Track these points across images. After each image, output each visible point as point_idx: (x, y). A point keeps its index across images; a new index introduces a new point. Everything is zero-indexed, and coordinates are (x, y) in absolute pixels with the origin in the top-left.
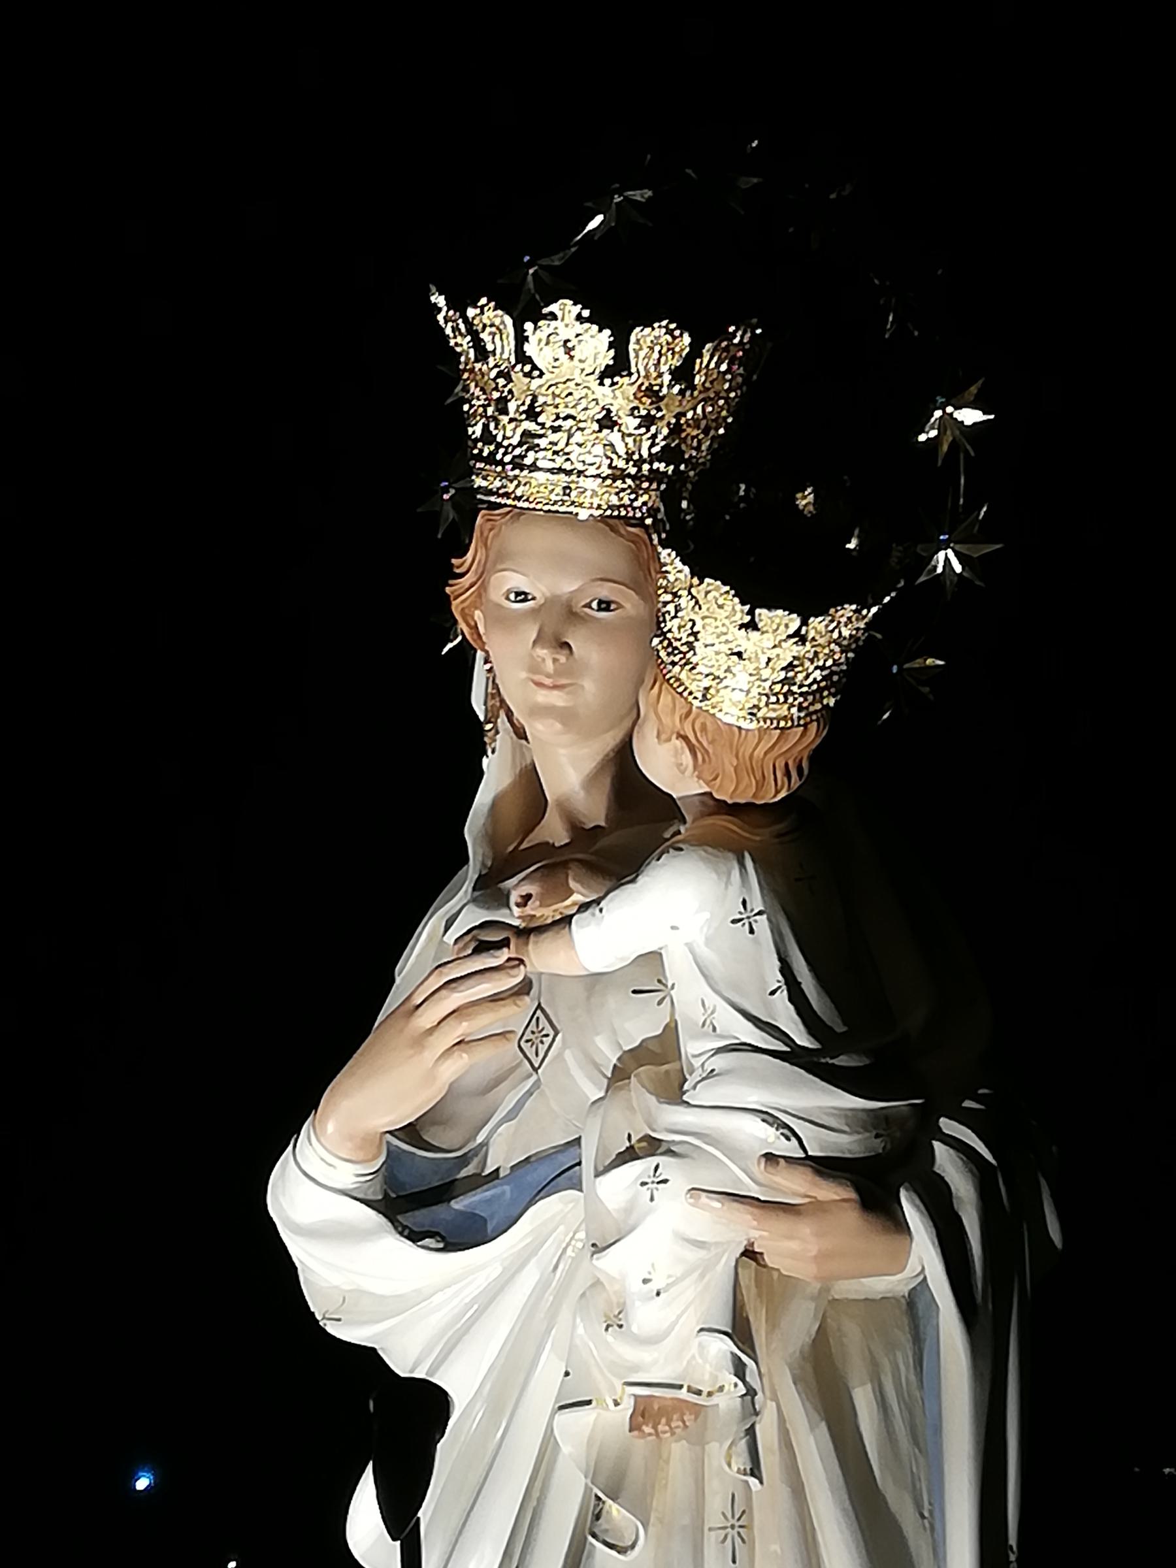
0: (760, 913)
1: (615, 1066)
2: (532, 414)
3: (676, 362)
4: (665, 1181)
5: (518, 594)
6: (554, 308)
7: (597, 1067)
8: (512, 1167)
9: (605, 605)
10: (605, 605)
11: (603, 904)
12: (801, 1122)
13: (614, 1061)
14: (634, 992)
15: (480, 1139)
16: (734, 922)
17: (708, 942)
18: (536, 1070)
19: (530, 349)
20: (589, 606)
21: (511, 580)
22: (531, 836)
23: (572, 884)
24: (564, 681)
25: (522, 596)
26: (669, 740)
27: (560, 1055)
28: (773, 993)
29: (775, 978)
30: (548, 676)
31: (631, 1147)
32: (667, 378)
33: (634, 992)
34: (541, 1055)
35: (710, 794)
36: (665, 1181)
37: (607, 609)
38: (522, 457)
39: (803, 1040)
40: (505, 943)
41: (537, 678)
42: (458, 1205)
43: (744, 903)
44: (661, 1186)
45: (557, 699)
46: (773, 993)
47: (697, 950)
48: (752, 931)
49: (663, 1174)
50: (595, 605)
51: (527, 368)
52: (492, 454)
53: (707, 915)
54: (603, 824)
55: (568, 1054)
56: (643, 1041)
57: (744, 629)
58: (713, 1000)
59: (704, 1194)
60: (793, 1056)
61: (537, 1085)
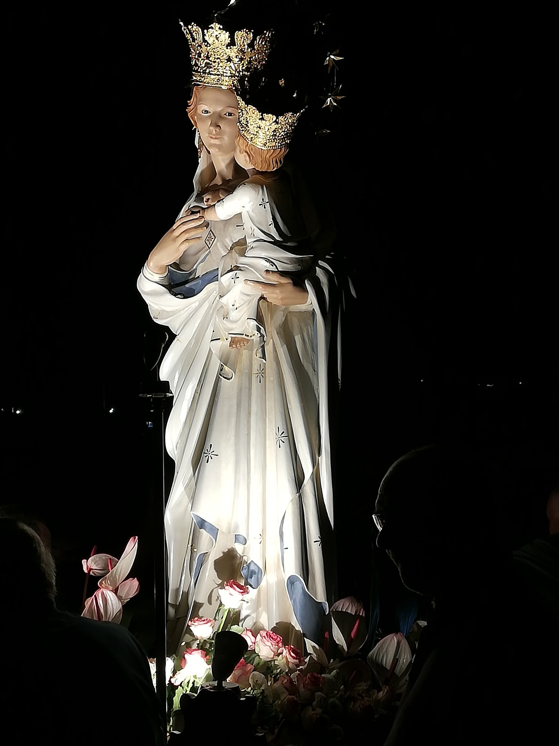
0: (267, 202)
1: (231, 247)
3: (249, 42)
4: (238, 278)
6: (212, 25)
7: (226, 247)
8: (202, 275)
9: (230, 114)
10: (230, 114)
11: (224, 200)
13: (231, 245)
14: (237, 226)
15: (194, 268)
16: (260, 205)
18: (209, 248)
19: (206, 38)
20: (226, 114)
24: (218, 137)
25: (207, 112)
27: (216, 244)
28: (270, 225)
30: (214, 135)
32: (246, 46)
33: (237, 226)
34: (211, 244)
36: (238, 278)
37: (231, 116)
38: (205, 70)
39: (278, 238)
40: (199, 212)
41: (211, 136)
42: (187, 286)
43: (263, 199)
44: (238, 279)
45: (217, 142)
46: (270, 225)
47: (249, 213)
48: (265, 208)
50: (227, 114)
51: (206, 44)
52: (198, 69)
53: (252, 203)
54: (231, 178)
55: (218, 244)
59: (249, 281)
60: (275, 243)
61: (210, 252)
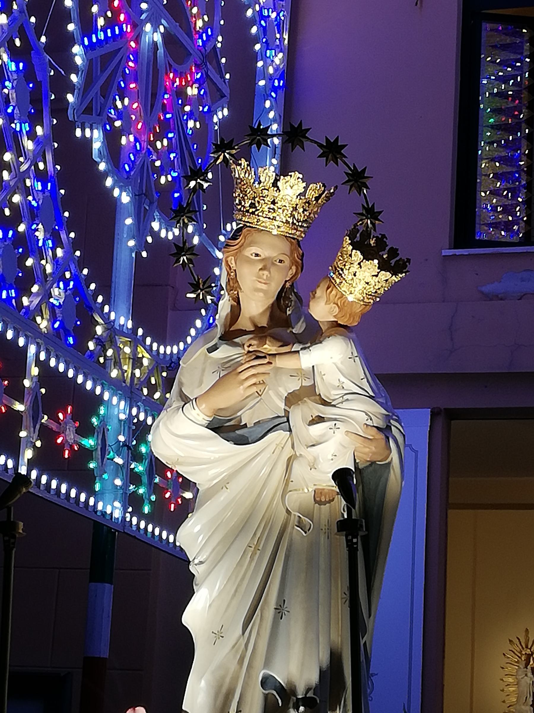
0: (356, 357)
1: (286, 397)
2: (274, 203)
3: (317, 195)
4: (339, 428)
5: (256, 254)
6: (293, 174)
7: (281, 396)
8: (254, 424)
9: (281, 261)
10: (281, 261)
11: (310, 348)
12: (282, 422)
13: (286, 395)
14: (291, 376)
15: (239, 414)
16: (350, 358)
17: (342, 363)
18: (261, 395)
19: (279, 184)
20: (276, 261)
21: (254, 249)
22: (233, 327)
23: (267, 342)
24: (268, 282)
25: (257, 255)
26: (330, 304)
27: (267, 392)
28: (362, 379)
29: (363, 376)
30: (264, 280)
31: (313, 419)
32: (313, 199)
33: (291, 376)
34: (262, 391)
35: (337, 322)
36: (339, 428)
37: (281, 263)
40: (265, 357)
41: (260, 280)
42: (238, 432)
43: (352, 353)
44: (337, 430)
45: (264, 287)
46: (362, 379)
47: (338, 365)
48: (355, 361)
49: (337, 426)
50: (278, 261)
51: (276, 189)
53: (342, 356)
54: (266, 325)
55: (270, 392)
56: (294, 391)
57: (394, 276)
58: (343, 379)
59: (350, 434)
60: (371, 397)
61: (261, 399)
